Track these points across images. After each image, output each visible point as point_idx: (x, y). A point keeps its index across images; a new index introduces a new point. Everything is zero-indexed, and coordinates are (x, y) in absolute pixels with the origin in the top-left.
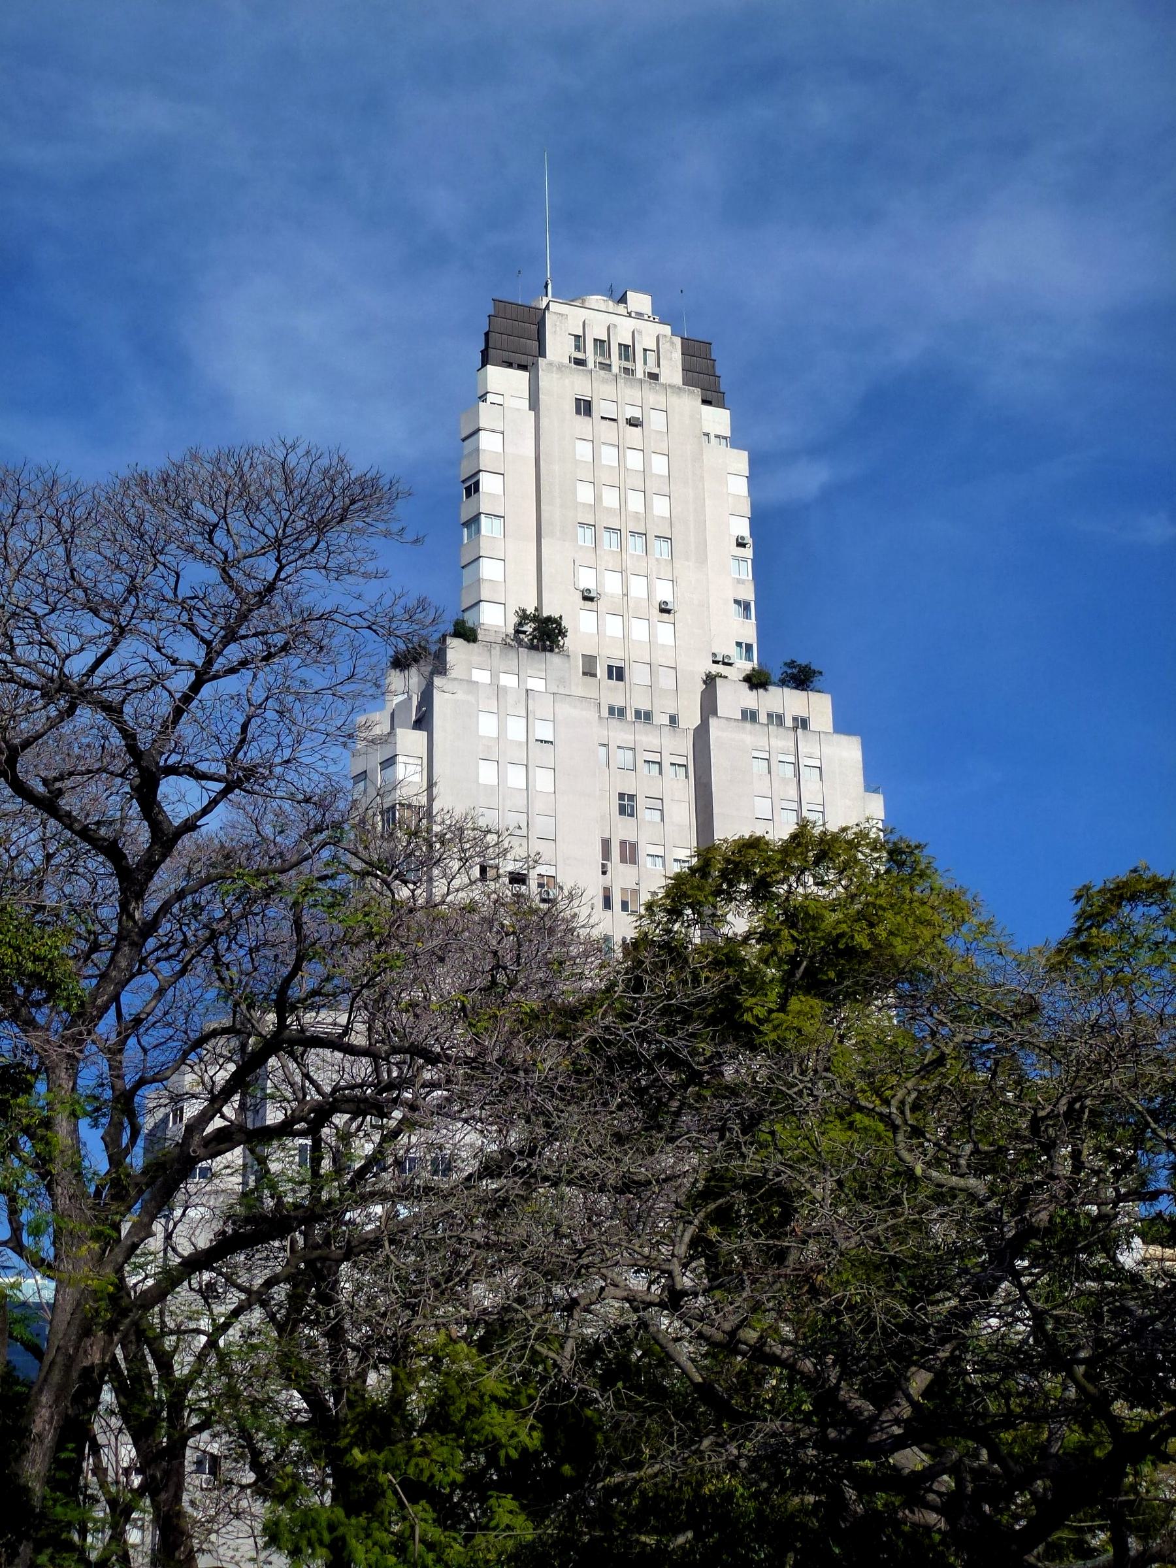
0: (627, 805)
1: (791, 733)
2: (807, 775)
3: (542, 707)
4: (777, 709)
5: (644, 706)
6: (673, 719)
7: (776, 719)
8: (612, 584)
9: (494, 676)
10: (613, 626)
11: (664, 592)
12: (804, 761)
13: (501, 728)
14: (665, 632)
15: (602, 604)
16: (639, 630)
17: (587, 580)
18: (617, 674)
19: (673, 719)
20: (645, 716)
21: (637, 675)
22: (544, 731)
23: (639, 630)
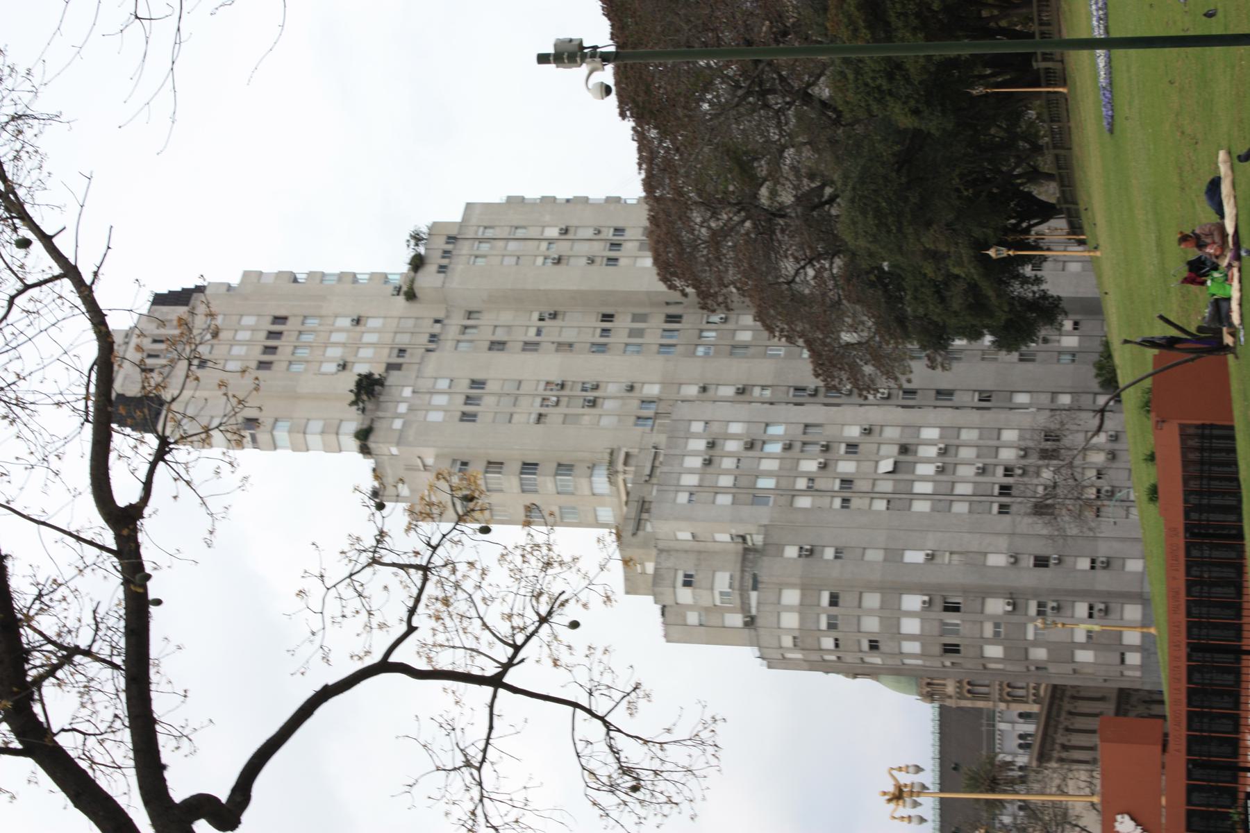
0: (497, 346)
1: (460, 242)
2: (490, 233)
3: (424, 384)
4: (440, 253)
5: (426, 337)
6: (437, 321)
7: (446, 254)
8: (335, 353)
9: (399, 416)
10: (365, 353)
11: (346, 322)
12: (480, 235)
13: (438, 408)
14: (372, 323)
15: (350, 359)
16: (370, 338)
17: (331, 367)
18: (402, 351)
19: (437, 321)
20: (433, 338)
21: (403, 340)
22: (443, 384)
23: (370, 338)
